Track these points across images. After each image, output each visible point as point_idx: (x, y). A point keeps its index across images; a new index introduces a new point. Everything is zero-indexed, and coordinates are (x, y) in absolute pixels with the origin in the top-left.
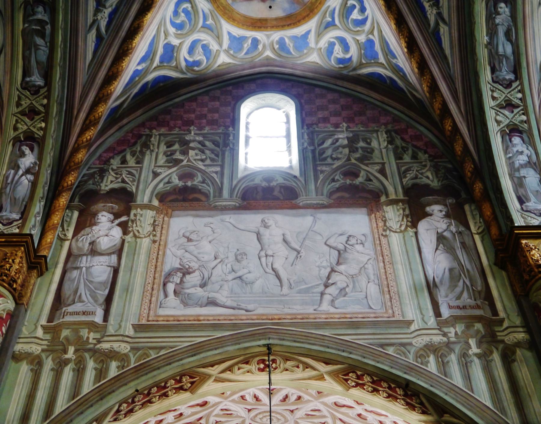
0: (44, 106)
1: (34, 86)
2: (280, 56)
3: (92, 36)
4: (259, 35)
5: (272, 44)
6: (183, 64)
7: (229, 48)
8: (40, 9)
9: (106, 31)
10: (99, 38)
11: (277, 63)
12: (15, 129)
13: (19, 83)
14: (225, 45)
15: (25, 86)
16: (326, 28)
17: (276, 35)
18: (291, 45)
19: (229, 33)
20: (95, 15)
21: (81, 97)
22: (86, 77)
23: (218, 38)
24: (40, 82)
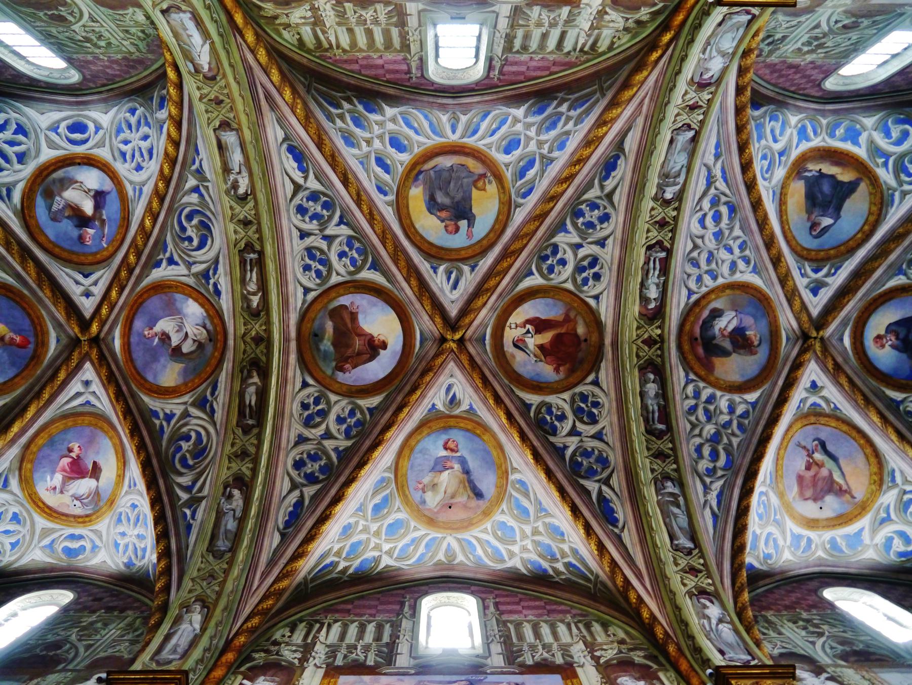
0: (703, 565)
1: (685, 548)
2: (832, 556)
3: (708, 513)
4: (812, 534)
5: (824, 543)
6: (762, 555)
7: (791, 544)
8: (669, 484)
9: (719, 509)
10: (715, 516)
11: (830, 563)
12: (685, 585)
13: (669, 545)
14: (788, 543)
15: (677, 548)
16: (881, 524)
17: (828, 535)
18: (844, 544)
19: (791, 530)
20: (705, 496)
21: (717, 565)
22: (715, 549)
23: (783, 533)
24: (690, 545)
